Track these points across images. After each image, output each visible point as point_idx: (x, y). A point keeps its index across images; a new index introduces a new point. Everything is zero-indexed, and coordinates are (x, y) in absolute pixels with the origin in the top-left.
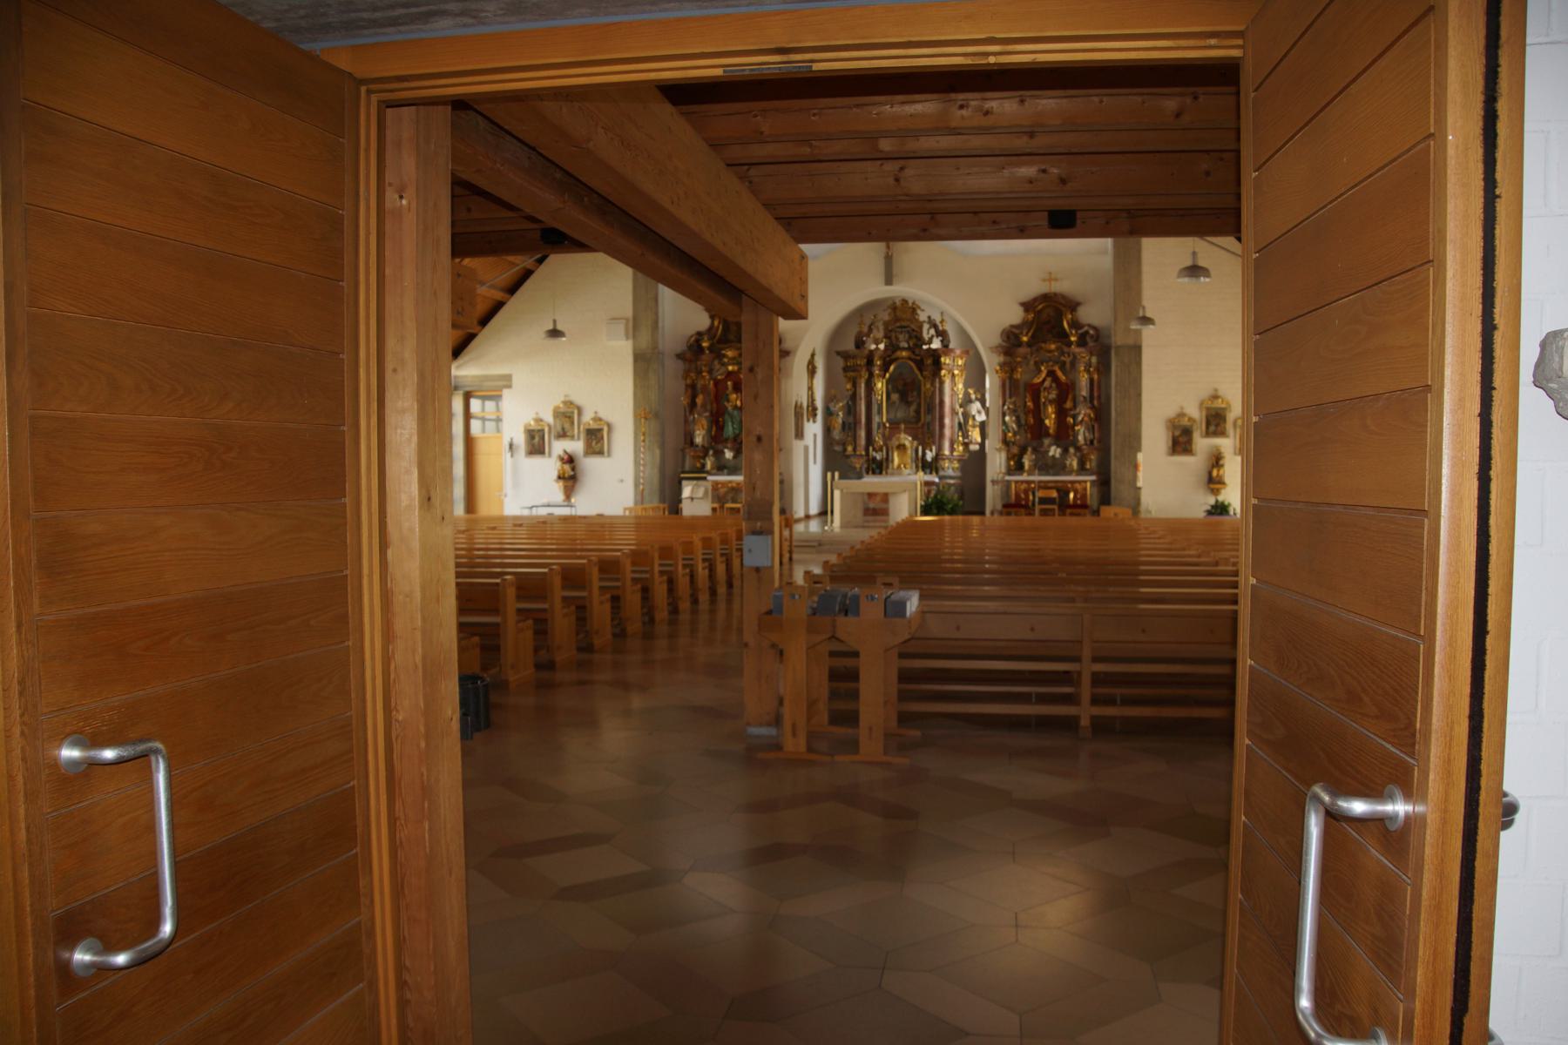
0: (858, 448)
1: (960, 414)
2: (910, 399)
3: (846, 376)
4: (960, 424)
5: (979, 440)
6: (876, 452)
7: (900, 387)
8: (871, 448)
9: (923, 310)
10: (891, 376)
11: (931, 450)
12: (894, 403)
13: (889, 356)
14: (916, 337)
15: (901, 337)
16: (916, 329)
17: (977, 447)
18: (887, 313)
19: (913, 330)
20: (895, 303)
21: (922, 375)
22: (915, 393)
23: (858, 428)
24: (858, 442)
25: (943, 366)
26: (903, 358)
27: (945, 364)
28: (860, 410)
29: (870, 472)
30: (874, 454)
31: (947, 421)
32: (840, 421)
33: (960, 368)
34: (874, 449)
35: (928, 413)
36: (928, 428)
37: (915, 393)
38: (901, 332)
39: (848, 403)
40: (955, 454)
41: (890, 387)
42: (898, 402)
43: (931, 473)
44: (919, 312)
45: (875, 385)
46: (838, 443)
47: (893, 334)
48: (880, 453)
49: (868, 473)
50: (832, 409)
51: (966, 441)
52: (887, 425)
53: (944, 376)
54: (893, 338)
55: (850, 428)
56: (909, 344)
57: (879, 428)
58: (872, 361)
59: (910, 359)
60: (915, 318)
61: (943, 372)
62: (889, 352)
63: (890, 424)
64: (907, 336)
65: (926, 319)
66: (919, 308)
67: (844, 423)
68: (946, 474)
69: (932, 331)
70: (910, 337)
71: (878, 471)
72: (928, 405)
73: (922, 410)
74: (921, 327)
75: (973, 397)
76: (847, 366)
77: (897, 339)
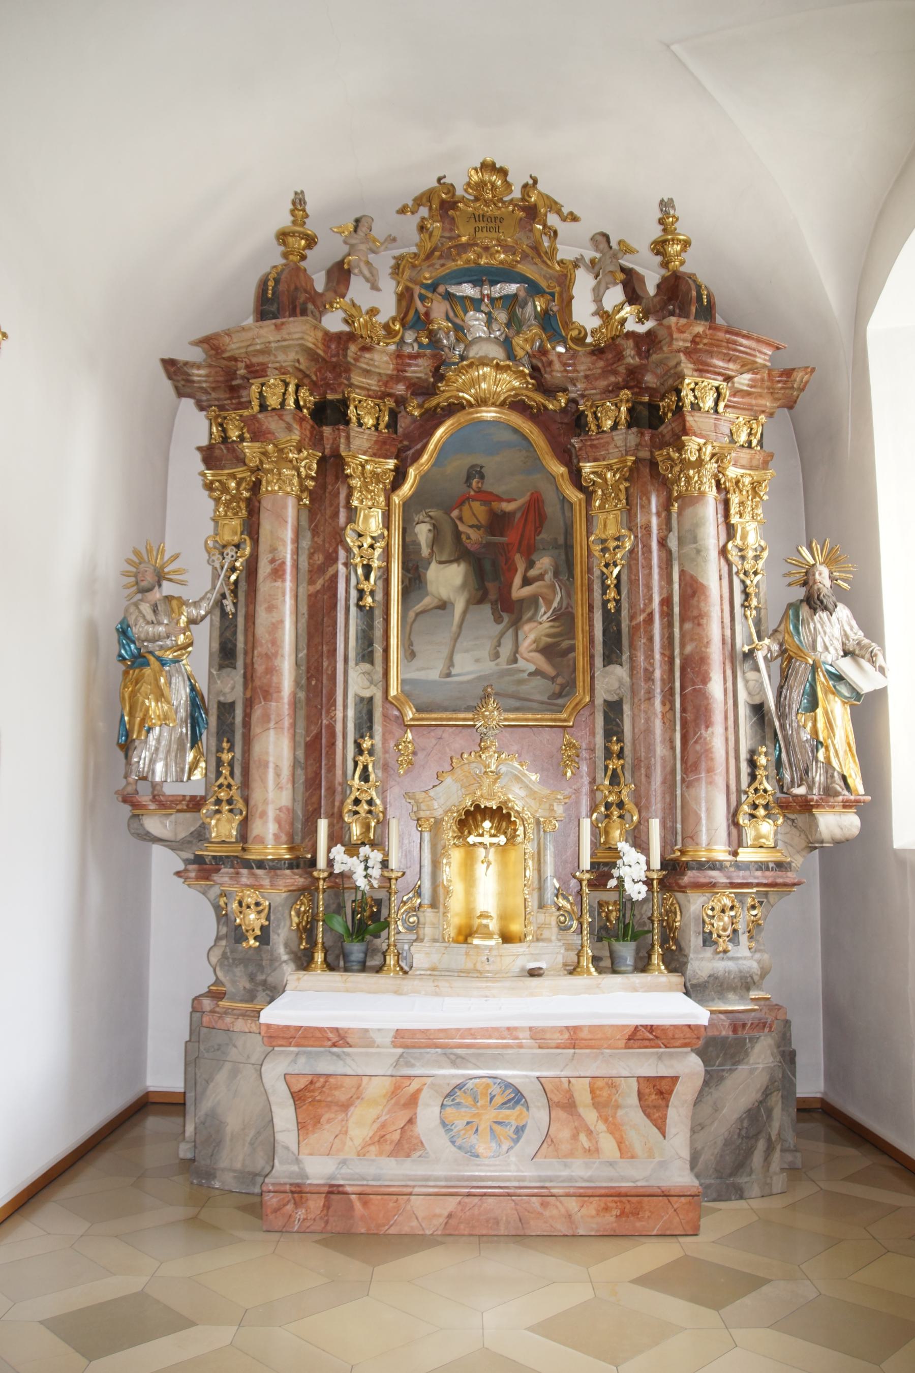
0: (256, 828)
1: (760, 656)
2: (519, 592)
3: (209, 487)
4: (759, 710)
5: (856, 782)
6: (352, 850)
7: (473, 537)
8: (323, 825)
9: (574, 218)
10: (424, 479)
11: (640, 843)
12: (444, 606)
13: (424, 390)
14: (546, 320)
15: (476, 322)
16: (543, 284)
17: (850, 823)
18: (412, 221)
19: (534, 289)
20: (451, 189)
21: (576, 476)
22: (544, 563)
23: (257, 713)
24: (256, 796)
25: (692, 420)
26: (482, 402)
27: (695, 407)
28: (277, 626)
29: (319, 957)
30: (338, 851)
31: (716, 688)
32: (180, 695)
33: (745, 455)
34: (337, 836)
35: (612, 655)
36: (613, 729)
37: (544, 563)
38: (476, 304)
39: (219, 604)
40: (746, 855)
41: (423, 532)
42: (459, 606)
43: (643, 965)
44: (553, 220)
45: (352, 514)
46: (164, 804)
47: (439, 309)
48: (376, 857)
49: (304, 962)
50: (140, 629)
51: (801, 791)
52: (410, 714)
53: (700, 463)
54: (440, 322)
55: (225, 731)
56: (507, 344)
57: (365, 724)
58: (344, 403)
59: (517, 405)
60: (536, 248)
61: (692, 444)
62: (419, 370)
63: (418, 710)
64: (502, 316)
65: (590, 254)
66: (554, 206)
67: (196, 701)
68: (721, 966)
69: (614, 296)
70: (514, 322)
71: (356, 950)
72: (611, 620)
73: (580, 641)
74: (565, 281)
75: (823, 577)
76: (225, 439)
77: (460, 329)
